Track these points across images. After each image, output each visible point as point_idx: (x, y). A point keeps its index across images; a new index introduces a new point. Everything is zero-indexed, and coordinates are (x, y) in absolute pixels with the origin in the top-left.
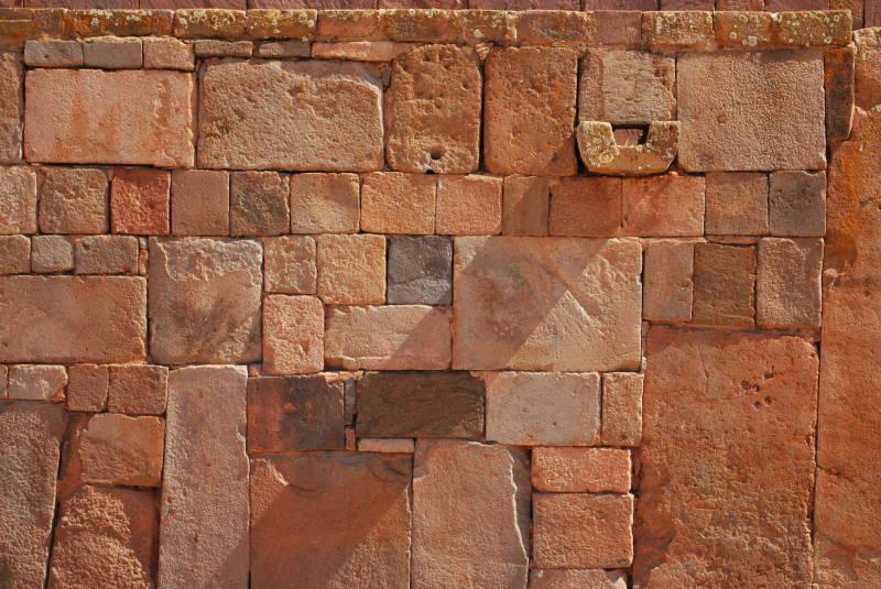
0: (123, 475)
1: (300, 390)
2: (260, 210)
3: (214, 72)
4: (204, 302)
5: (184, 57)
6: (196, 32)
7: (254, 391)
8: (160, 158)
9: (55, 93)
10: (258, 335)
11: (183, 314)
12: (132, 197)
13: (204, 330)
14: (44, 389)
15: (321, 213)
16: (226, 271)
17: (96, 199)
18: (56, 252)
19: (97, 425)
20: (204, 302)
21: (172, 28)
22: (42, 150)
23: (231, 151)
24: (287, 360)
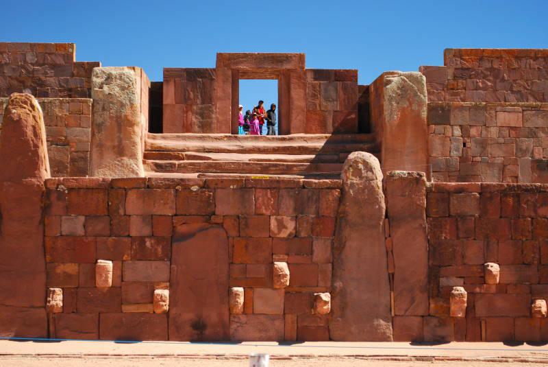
0: (513, 175)
1: (539, 161)
2: (532, 134)
3: (525, 113)
4: (524, 148)
5: (521, 110)
6: (522, 106)
7: (532, 161)
8: (517, 126)
9: (501, 116)
10: (532, 153)
11: (521, 150)
12: (513, 132)
13: (525, 152)
14: (499, 162)
15: (542, 135)
16: (527, 143)
17: (508, 131)
18: (502, 140)
19: (508, 167)
20: (524, 148)
21: (519, 106)
22: (499, 124)
23: (528, 125)
24: (537, 157)
